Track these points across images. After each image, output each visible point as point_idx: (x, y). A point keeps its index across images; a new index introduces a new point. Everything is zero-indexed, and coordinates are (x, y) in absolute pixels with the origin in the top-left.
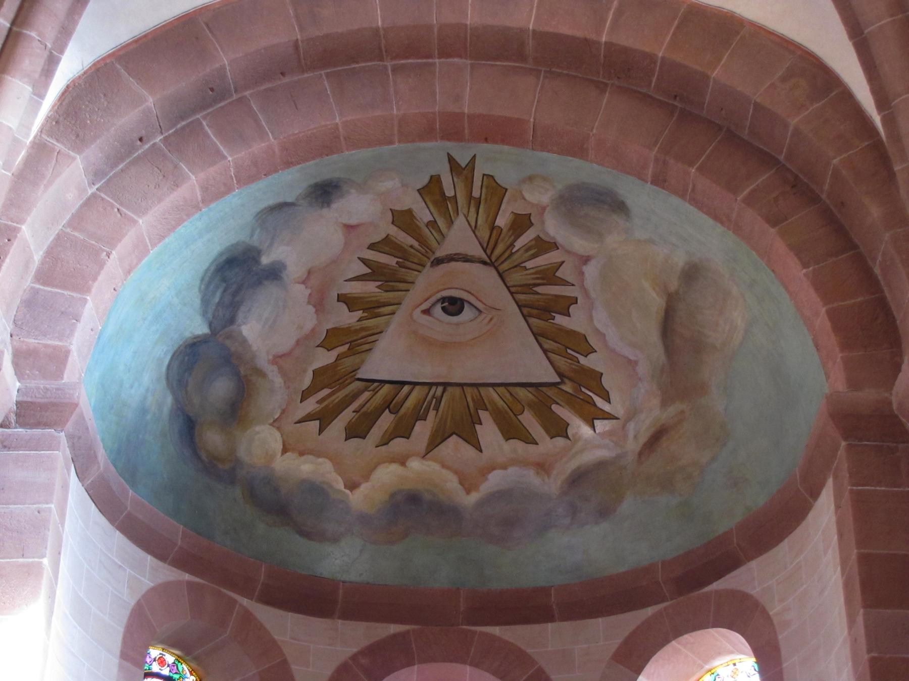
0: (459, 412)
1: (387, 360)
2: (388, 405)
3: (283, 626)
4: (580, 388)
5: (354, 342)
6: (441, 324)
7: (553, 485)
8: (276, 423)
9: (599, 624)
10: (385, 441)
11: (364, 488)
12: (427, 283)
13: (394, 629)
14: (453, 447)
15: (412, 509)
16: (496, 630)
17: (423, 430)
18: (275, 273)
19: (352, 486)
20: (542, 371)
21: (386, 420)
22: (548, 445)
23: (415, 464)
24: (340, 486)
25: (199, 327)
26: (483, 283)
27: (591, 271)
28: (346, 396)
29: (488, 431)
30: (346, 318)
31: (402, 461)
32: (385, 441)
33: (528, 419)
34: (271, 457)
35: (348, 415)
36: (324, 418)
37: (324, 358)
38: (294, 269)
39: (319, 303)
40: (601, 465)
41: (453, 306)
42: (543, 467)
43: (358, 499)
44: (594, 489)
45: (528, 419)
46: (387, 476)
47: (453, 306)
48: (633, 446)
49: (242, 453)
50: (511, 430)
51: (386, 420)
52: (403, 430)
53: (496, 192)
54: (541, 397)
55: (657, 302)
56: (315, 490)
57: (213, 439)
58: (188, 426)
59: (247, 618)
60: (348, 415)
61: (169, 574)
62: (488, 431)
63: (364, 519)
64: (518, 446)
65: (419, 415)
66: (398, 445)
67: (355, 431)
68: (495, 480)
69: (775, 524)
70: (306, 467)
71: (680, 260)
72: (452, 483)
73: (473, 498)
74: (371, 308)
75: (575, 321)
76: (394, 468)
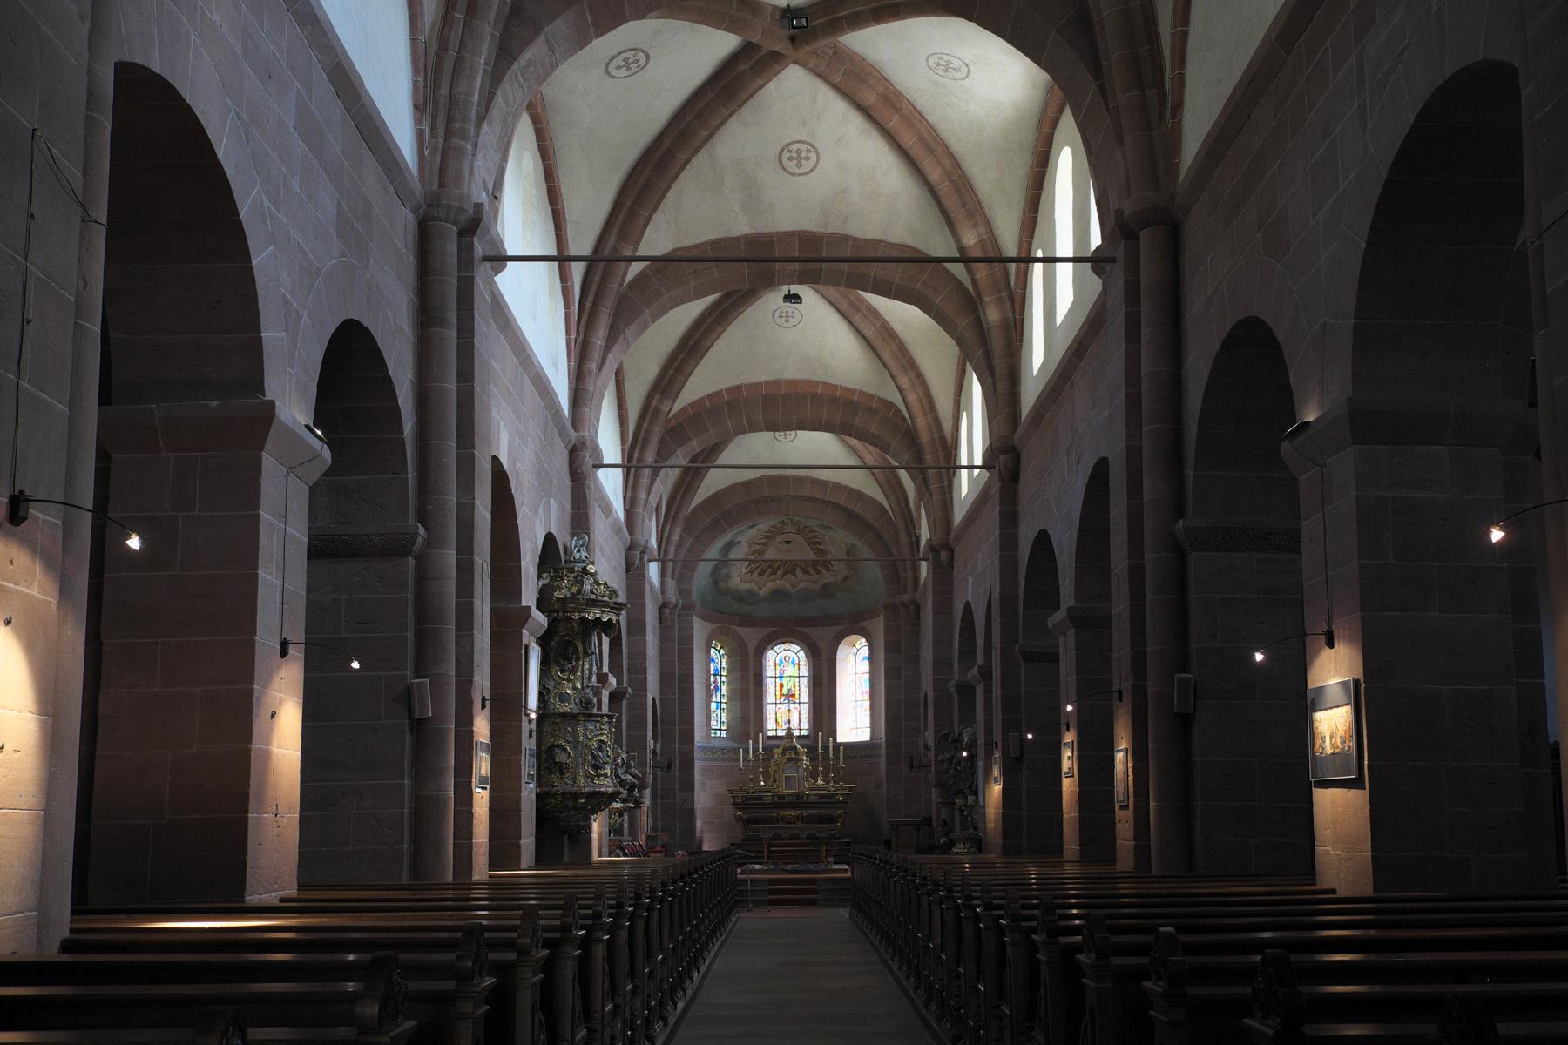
0: (790, 568)
1: (770, 554)
3: (743, 631)
4: (827, 565)
5: (760, 553)
7: (817, 587)
12: (780, 538)
14: (789, 576)
15: (777, 594)
17: (780, 572)
20: (813, 556)
26: (798, 538)
28: (761, 567)
29: (799, 572)
36: (751, 572)
41: (788, 542)
44: (827, 591)
46: (770, 585)
47: (788, 542)
50: (805, 572)
52: (774, 573)
54: (814, 564)
56: (750, 592)
57: (722, 585)
58: (716, 583)
61: (715, 625)
62: (799, 572)
67: (760, 574)
68: (802, 585)
69: (871, 614)
70: (747, 586)
72: (788, 586)
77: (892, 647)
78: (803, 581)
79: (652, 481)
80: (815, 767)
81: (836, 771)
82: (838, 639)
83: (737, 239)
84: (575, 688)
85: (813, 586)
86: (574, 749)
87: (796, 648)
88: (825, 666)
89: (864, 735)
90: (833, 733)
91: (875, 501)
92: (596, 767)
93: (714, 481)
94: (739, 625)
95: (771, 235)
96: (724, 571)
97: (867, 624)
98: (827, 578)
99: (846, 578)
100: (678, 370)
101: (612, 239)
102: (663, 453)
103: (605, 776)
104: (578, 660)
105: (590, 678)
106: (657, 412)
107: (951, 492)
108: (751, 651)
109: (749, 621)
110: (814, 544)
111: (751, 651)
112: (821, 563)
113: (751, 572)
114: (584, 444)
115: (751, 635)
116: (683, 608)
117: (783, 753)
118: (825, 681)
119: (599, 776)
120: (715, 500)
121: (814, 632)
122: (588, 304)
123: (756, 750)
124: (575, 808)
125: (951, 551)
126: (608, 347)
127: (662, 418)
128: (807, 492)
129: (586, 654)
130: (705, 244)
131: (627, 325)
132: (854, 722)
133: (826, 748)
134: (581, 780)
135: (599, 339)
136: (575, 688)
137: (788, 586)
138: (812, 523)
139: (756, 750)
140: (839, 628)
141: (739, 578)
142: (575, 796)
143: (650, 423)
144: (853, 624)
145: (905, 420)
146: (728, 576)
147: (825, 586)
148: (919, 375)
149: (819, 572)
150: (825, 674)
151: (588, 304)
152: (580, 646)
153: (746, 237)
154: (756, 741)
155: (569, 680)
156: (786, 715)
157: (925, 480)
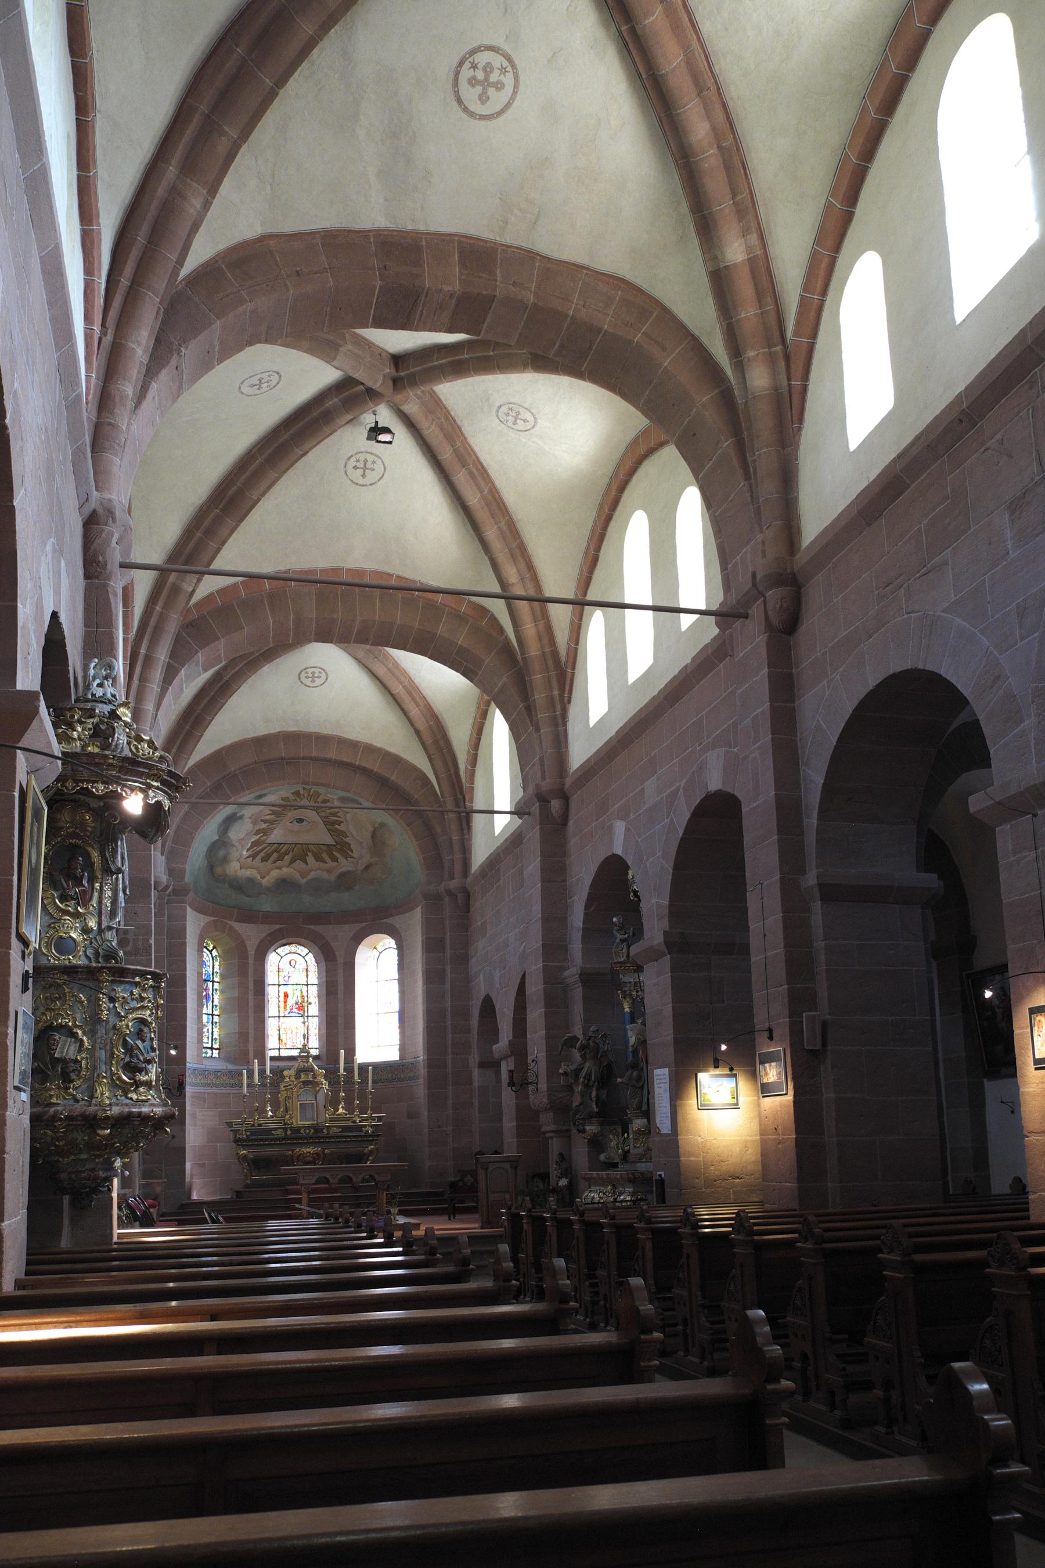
0: (300, 853)
1: (277, 836)
2: (275, 851)
5: (265, 832)
6: (296, 826)
7: (332, 877)
8: (238, 860)
9: (347, 927)
10: (275, 862)
11: (267, 878)
12: (292, 814)
13: (278, 927)
14: (298, 864)
15: (284, 885)
16: (312, 927)
17: (288, 858)
18: (241, 817)
19: (263, 877)
20: (330, 841)
21: (275, 855)
22: (331, 864)
23: (285, 870)
24: (259, 877)
25: (216, 838)
26: (312, 815)
27: (349, 816)
29: (310, 859)
30: (264, 826)
31: (280, 868)
32: (275, 862)
33: (325, 856)
34: (236, 871)
35: (262, 854)
37: (255, 838)
38: (247, 816)
39: (254, 823)
40: (349, 872)
42: (329, 871)
43: (265, 882)
44: (345, 882)
45: (325, 856)
46: (275, 873)
48: (360, 867)
49: (228, 872)
50: (318, 858)
51: (275, 855)
52: (281, 858)
53: (318, 794)
55: (371, 829)
56: (251, 881)
57: (219, 870)
58: (211, 868)
59: (231, 927)
60: (262, 854)
62: (310, 859)
63: (268, 889)
64: (321, 864)
65: (286, 853)
66: (279, 863)
67: (263, 860)
69: (403, 907)
70: (248, 873)
71: (379, 820)
72: (297, 875)
73: (305, 880)
74: (272, 822)
75: (342, 828)
76: (277, 871)
77: (433, 946)
78: (315, 869)
79: (164, 691)
80: (335, 1093)
81: (362, 1096)
82: (358, 939)
83: (364, 234)
84: (86, 930)
85: (325, 876)
86: (92, 1034)
87: (304, 951)
88: (340, 971)
89: (392, 1055)
90: (351, 1052)
91: (415, 768)
92: (132, 1069)
93: (225, 729)
94: (237, 921)
95: (417, 235)
96: (222, 853)
97: (396, 921)
98: (345, 865)
99: (368, 867)
100: (210, 532)
101: (172, 171)
102: (179, 657)
103: (148, 1084)
104: (92, 880)
105: (113, 914)
106: (176, 590)
107: (565, 723)
108: (251, 952)
109: (249, 916)
110: (331, 824)
111: (251, 952)
112: (341, 847)
113: (253, 856)
114: (110, 512)
115: (251, 934)
116: (176, 892)
117: (298, 1076)
118: (341, 988)
119: (138, 1084)
120: (218, 758)
121: (328, 931)
122: (124, 281)
123: (262, 1072)
124: (91, 1146)
125: (565, 798)
126: (151, 371)
127: (182, 599)
128: (332, 755)
129: (107, 871)
130: (312, 234)
131: (184, 341)
132: (379, 1035)
133: (349, 1070)
134: (104, 1093)
135: (140, 345)
136: (86, 930)
137: (297, 875)
138: (334, 796)
139: (262, 1072)
140: (357, 927)
141: (239, 864)
142: (92, 1122)
143: (167, 605)
144: (376, 920)
145: (502, 630)
146: (225, 860)
147: (342, 875)
148: (530, 567)
149: (335, 859)
150: (341, 979)
151: (124, 281)
152: (95, 856)
153: (378, 233)
154: (262, 1063)
155: (76, 915)
156: (291, 1030)
157: (529, 709)
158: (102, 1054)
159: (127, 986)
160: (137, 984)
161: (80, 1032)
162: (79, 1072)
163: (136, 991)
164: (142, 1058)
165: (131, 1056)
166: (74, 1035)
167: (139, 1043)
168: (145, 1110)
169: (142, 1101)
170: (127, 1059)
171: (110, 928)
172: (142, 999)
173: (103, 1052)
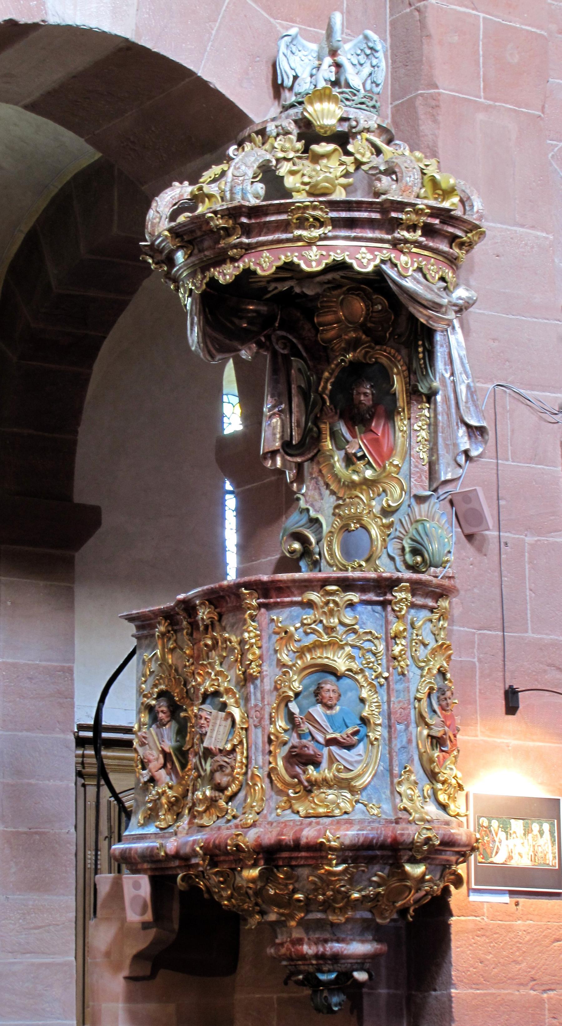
158: (258, 737)
159: (296, 610)
160: (310, 604)
161: (231, 701)
162: (233, 768)
163: (309, 616)
164: (320, 738)
165: (300, 736)
166: (224, 707)
167: (318, 711)
168: (309, 834)
169: (318, 816)
170: (294, 740)
171: (420, 499)
172: (329, 630)
173: (259, 731)
